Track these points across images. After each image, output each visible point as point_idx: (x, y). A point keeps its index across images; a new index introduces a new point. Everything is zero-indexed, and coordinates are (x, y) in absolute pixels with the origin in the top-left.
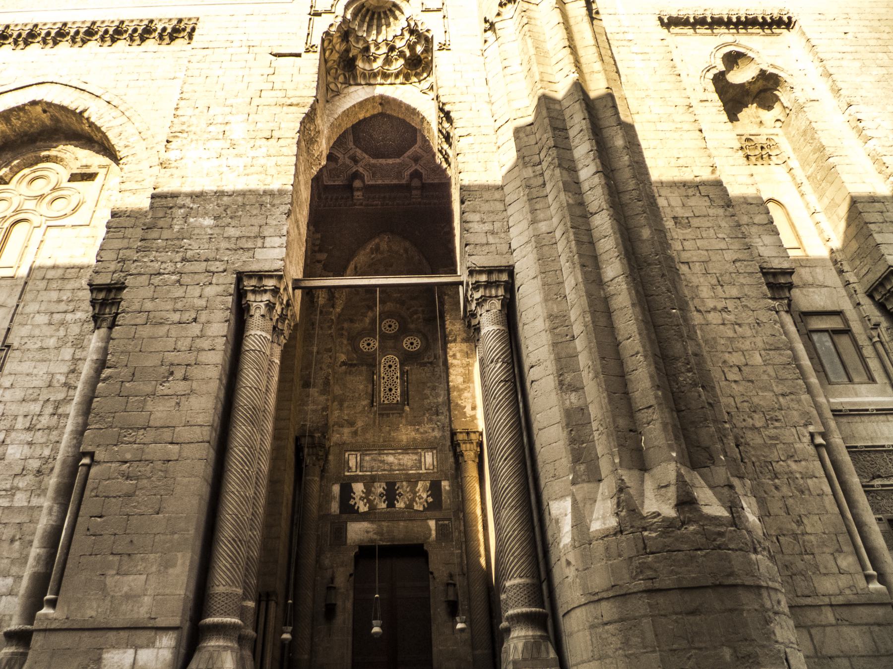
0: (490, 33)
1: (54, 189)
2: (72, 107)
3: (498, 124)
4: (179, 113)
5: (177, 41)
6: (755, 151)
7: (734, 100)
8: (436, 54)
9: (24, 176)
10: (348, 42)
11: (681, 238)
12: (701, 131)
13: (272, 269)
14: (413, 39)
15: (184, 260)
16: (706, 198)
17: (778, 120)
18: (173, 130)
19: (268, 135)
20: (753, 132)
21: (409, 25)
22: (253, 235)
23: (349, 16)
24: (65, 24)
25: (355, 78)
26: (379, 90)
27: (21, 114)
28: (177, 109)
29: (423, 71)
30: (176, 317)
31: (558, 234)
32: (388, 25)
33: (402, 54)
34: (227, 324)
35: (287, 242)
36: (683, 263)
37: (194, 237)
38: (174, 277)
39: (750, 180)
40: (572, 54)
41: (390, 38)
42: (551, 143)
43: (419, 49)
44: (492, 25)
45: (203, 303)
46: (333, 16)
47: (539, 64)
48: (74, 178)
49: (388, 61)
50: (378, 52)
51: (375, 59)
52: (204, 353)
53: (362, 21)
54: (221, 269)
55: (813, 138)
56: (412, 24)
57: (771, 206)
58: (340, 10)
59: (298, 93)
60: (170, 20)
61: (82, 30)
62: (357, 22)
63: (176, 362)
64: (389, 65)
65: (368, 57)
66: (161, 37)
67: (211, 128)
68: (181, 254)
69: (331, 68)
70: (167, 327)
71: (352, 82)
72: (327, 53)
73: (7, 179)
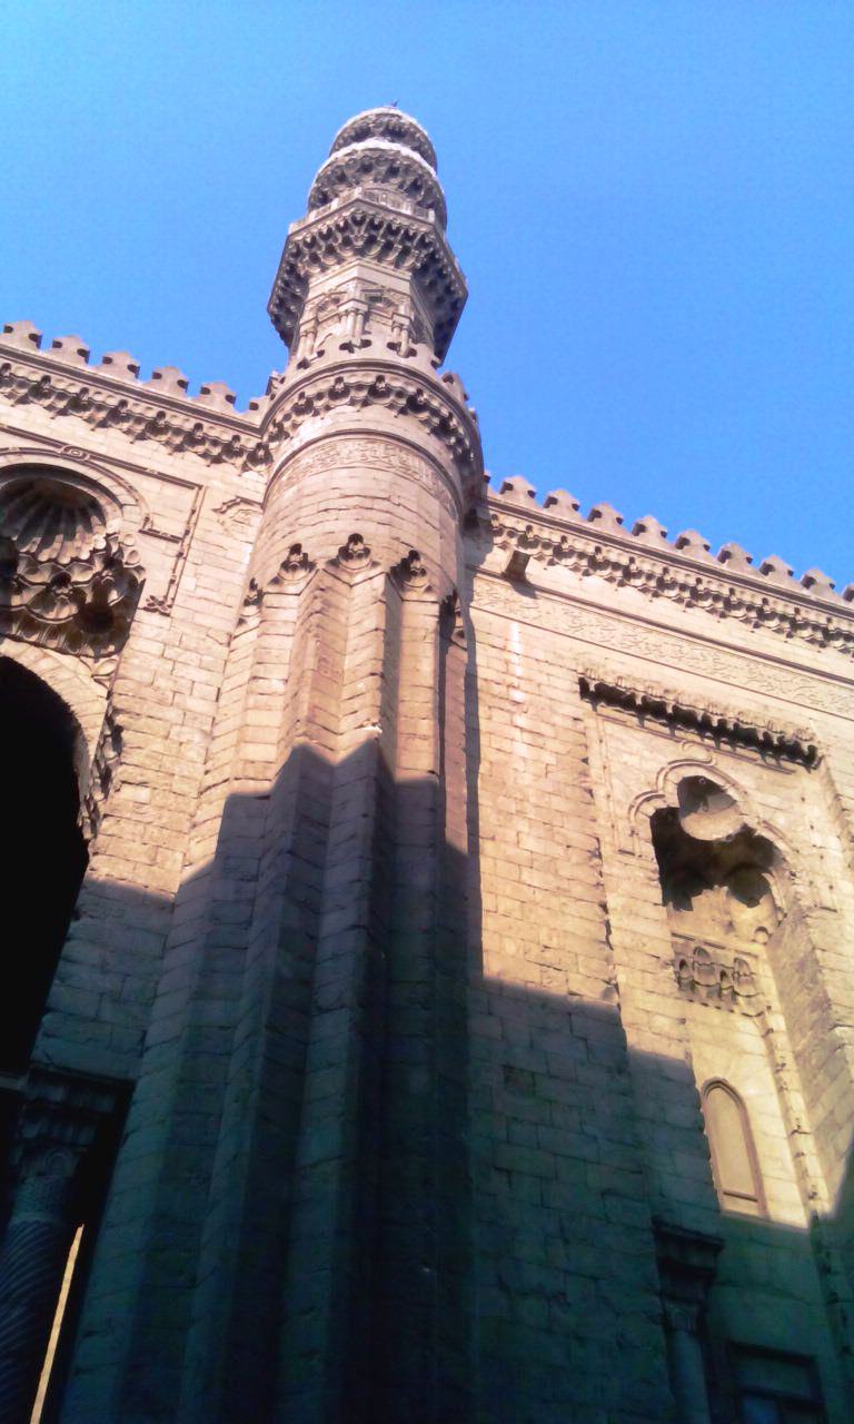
0: (252, 610)
3: (209, 780)
6: (703, 977)
7: (686, 867)
8: (140, 615)
12: (604, 907)
14: (108, 575)
16: (581, 1044)
17: (762, 929)
20: (712, 939)
21: (108, 548)
29: (110, 641)
31: (240, 1034)
32: (70, 536)
33: (77, 596)
36: (499, 1170)
39: (677, 1031)
40: (382, 689)
41: (65, 560)
42: (287, 843)
43: (114, 596)
44: (261, 595)
47: (314, 689)
49: (46, 598)
51: (21, 588)
53: (20, 512)
55: (814, 981)
56: (115, 549)
57: (716, 1103)
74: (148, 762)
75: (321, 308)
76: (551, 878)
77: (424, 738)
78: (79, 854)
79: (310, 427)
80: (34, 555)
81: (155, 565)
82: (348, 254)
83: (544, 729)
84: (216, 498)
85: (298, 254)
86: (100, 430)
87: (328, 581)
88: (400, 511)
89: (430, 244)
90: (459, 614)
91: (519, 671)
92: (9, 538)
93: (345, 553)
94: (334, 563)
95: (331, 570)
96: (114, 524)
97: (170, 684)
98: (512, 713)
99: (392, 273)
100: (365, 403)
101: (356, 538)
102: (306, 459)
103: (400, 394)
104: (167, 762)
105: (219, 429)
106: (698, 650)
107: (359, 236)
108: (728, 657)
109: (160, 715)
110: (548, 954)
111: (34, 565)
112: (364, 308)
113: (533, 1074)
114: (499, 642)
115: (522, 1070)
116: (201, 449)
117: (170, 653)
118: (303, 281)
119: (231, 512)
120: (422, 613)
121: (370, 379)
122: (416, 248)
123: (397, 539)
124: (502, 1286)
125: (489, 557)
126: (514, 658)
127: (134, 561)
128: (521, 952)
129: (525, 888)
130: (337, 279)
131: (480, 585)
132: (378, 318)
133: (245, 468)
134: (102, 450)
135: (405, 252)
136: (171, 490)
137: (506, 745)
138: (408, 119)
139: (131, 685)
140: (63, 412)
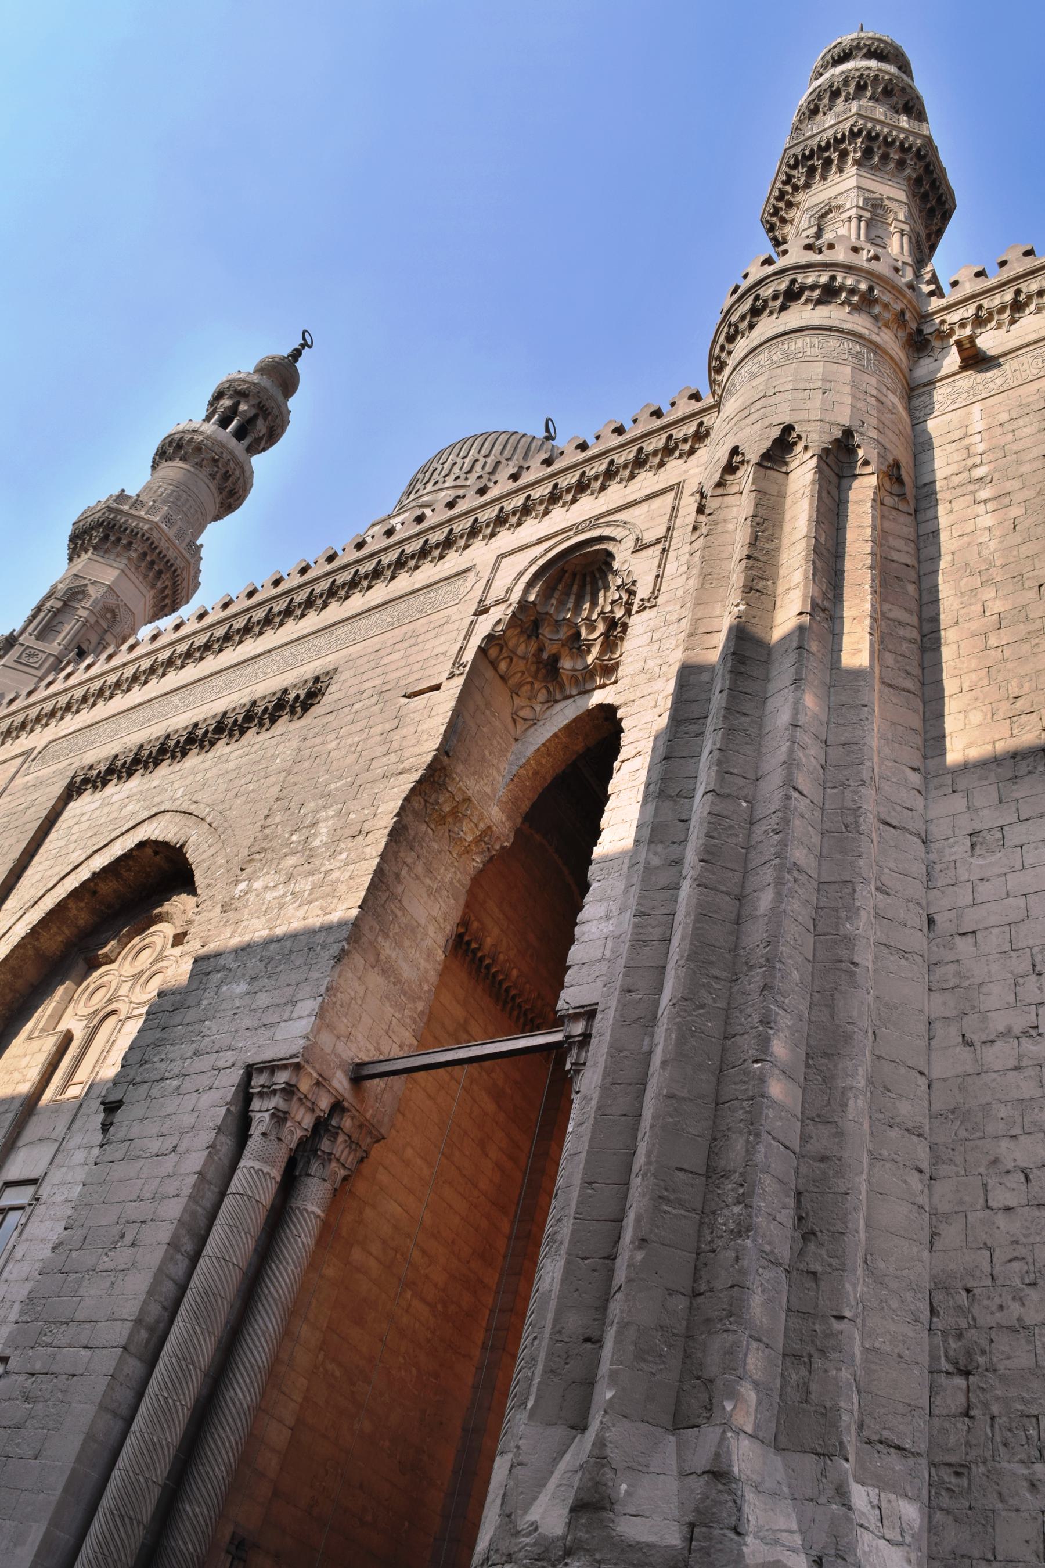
1: (155, 961)
2: (173, 842)
5: (313, 709)
9: (134, 947)
10: (537, 637)
11: (975, 877)
13: (287, 1055)
18: (253, 850)
19: (354, 830)
22: (284, 1000)
24: (196, 725)
25: (562, 688)
26: (598, 698)
27: (131, 863)
28: (267, 817)
30: (155, 1146)
32: (607, 588)
34: (206, 1152)
35: (322, 1007)
37: (218, 1015)
38: (176, 1083)
41: (608, 608)
45: (189, 1120)
46: (505, 605)
51: (589, 648)
52: (166, 1201)
54: (229, 1064)
59: (416, 750)
60: (306, 681)
61: (211, 728)
62: (554, 601)
63: (133, 1218)
64: (613, 652)
65: (579, 649)
67: (294, 838)
68: (194, 1045)
69: (520, 685)
70: (142, 1162)
71: (558, 697)
72: (503, 666)
73: (112, 956)
74: (641, 734)
76: (1021, 626)
77: (797, 586)
82: (800, 197)
83: (1009, 486)
86: (602, 494)
89: (860, 131)
90: (859, 446)
91: (981, 448)
92: (564, 619)
93: (730, 469)
94: (720, 484)
95: (720, 491)
96: (623, 557)
97: (659, 661)
98: (973, 493)
99: (839, 180)
101: (735, 451)
103: (775, 297)
105: (685, 428)
107: (800, 175)
109: (650, 691)
110: (1019, 703)
111: (592, 628)
112: (815, 229)
113: (1002, 827)
114: (957, 435)
115: (990, 830)
116: (677, 454)
117: (657, 635)
120: (802, 473)
122: (850, 144)
123: (770, 426)
124: (967, 1043)
125: (947, 362)
128: (989, 715)
129: (992, 652)
131: (940, 394)
132: (831, 228)
134: (604, 509)
135: (844, 154)
136: (657, 503)
137: (969, 527)
138: (846, 39)
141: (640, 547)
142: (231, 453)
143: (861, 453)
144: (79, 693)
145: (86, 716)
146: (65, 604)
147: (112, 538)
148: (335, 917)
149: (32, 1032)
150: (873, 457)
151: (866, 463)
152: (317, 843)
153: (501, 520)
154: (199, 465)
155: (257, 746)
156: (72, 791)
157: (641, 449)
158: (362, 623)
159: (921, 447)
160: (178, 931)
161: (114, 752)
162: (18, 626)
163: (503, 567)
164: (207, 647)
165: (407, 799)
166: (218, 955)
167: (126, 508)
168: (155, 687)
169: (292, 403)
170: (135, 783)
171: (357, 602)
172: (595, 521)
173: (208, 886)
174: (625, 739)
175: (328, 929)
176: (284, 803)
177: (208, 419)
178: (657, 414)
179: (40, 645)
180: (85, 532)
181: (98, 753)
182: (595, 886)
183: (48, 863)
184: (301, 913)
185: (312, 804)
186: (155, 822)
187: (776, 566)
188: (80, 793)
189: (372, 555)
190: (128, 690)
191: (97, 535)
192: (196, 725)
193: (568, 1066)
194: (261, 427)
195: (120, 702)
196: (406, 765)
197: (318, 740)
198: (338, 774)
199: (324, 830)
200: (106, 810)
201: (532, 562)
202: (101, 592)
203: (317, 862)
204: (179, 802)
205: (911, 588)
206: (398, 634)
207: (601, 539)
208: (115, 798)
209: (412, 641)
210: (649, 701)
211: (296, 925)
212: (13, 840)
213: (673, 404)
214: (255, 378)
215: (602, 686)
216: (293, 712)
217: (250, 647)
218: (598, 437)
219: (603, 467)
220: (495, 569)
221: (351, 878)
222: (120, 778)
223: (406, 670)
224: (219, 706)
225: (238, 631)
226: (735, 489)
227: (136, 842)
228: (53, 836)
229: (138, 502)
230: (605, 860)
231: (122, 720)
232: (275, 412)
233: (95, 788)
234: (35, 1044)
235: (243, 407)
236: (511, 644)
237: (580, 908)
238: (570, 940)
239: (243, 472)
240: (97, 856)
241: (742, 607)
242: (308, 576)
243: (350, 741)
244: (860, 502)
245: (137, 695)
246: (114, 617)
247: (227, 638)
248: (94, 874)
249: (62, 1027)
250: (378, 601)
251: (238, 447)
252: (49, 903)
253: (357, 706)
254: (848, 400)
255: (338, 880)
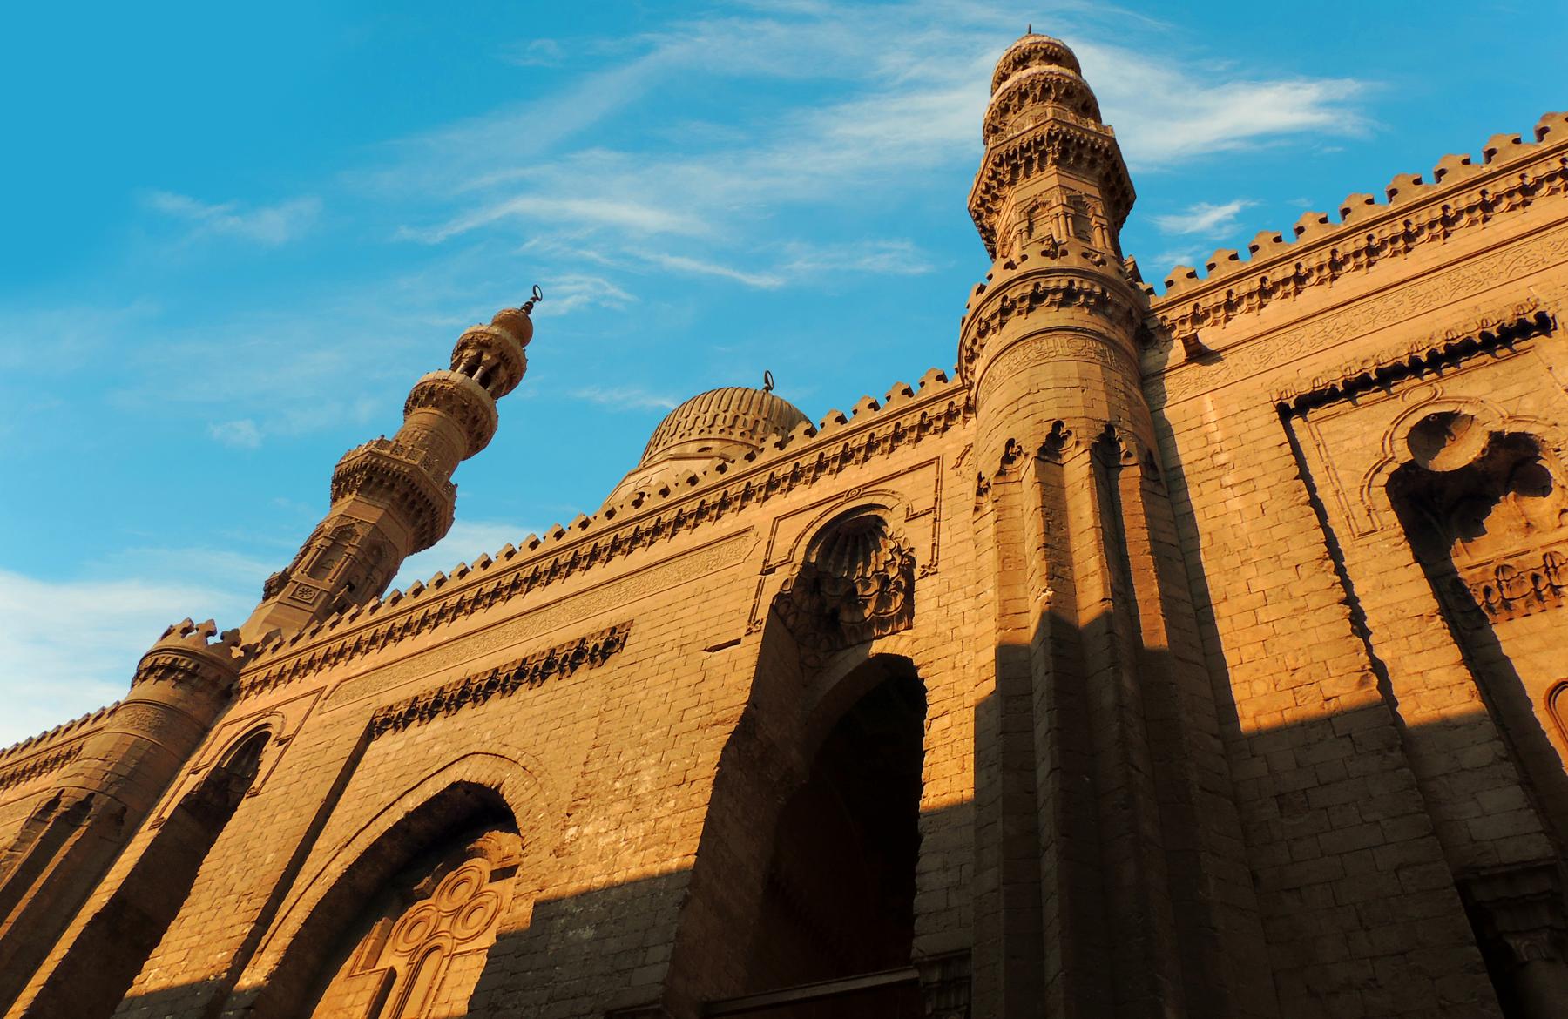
1: (474, 897)
4: (589, 768)
5: (611, 658)
15: (551, 999)
19: (679, 778)
23: (813, 559)
26: (877, 647)
28: (585, 764)
32: (878, 549)
48: (496, 876)
49: (884, 600)
50: (868, 593)
54: (588, 1010)
58: (799, 557)
59: (726, 703)
66: (593, 660)
67: (618, 785)
72: (790, 620)
75: (1003, 246)
77: (1095, 573)
78: (917, 787)
79: (979, 366)
80: (863, 576)
81: (917, 537)
84: (950, 461)
85: (979, 217)
87: (1000, 490)
88: (1039, 397)
93: (1008, 459)
94: (1001, 473)
95: (1001, 479)
97: (949, 625)
100: (1002, 324)
101: (1011, 443)
102: (981, 396)
103: (1022, 300)
104: (958, 688)
106: (1392, 297)
108: (1424, 285)
111: (866, 584)
116: (932, 429)
118: (992, 231)
119: (965, 461)
120: (1077, 466)
121: (996, 305)
126: (1213, 427)
127: (907, 547)
130: (1007, 217)
133: (965, 420)
134: (871, 479)
139: (921, 642)
140: (840, 469)
141: (912, 517)
142: (479, 400)
143: (1123, 446)
144: (367, 634)
145: (375, 657)
146: (334, 543)
147: (375, 480)
148: (674, 863)
149: (352, 970)
150: (1134, 451)
151: (1129, 455)
152: (641, 791)
153: (772, 485)
154: (450, 411)
155: (560, 693)
156: (373, 731)
157: (898, 425)
158: (648, 577)
159: (1163, 433)
160: (496, 867)
161: (412, 694)
162: (287, 563)
163: (783, 527)
164: (495, 594)
165: (724, 750)
166: (558, 900)
167: (387, 452)
168: (445, 631)
169: (530, 350)
170: (438, 724)
171: (641, 556)
172: (863, 490)
173: (532, 828)
174: (931, 698)
175: (667, 875)
176: (602, 750)
177: (454, 367)
178: (908, 392)
179: (312, 582)
180: (348, 474)
181: (397, 694)
182: (926, 838)
183: (357, 802)
184: (637, 859)
185: (631, 752)
186: (464, 765)
187: (1068, 552)
188: (381, 733)
189: (652, 513)
190: (418, 632)
191: (360, 478)
192: (496, 670)
193: (929, 1011)
194: (503, 373)
195: (409, 644)
196: (720, 716)
197: (625, 690)
198: (652, 723)
199: (647, 778)
200: (411, 751)
201: (810, 526)
202: (368, 530)
203: (646, 809)
204: (487, 745)
205: (1180, 566)
206: (688, 589)
207: (871, 507)
208: (419, 739)
209: (704, 597)
210: (947, 662)
211: (634, 872)
212: (317, 780)
213: (922, 384)
214: (496, 330)
215: (881, 637)
216: (593, 660)
217: (538, 595)
218: (855, 412)
219: (865, 440)
220: (774, 532)
221: (683, 825)
222: (422, 719)
223: (703, 625)
224: (518, 653)
225: (526, 580)
226: (1014, 478)
227: (448, 783)
228: (356, 775)
229: (398, 448)
230: (935, 813)
231: (416, 663)
232: (515, 361)
233: (396, 728)
234: (358, 983)
235: (486, 357)
236: (798, 599)
237: (915, 859)
238: (912, 890)
239: (489, 417)
240: (408, 796)
241: (1049, 593)
242: (590, 530)
243: (658, 692)
244: (1131, 491)
245: (427, 638)
246: (380, 552)
247: (515, 586)
248: (407, 814)
249: (384, 963)
250: (662, 557)
251: (483, 393)
252: (363, 843)
253: (659, 658)
254: (1103, 397)
255: (669, 828)
